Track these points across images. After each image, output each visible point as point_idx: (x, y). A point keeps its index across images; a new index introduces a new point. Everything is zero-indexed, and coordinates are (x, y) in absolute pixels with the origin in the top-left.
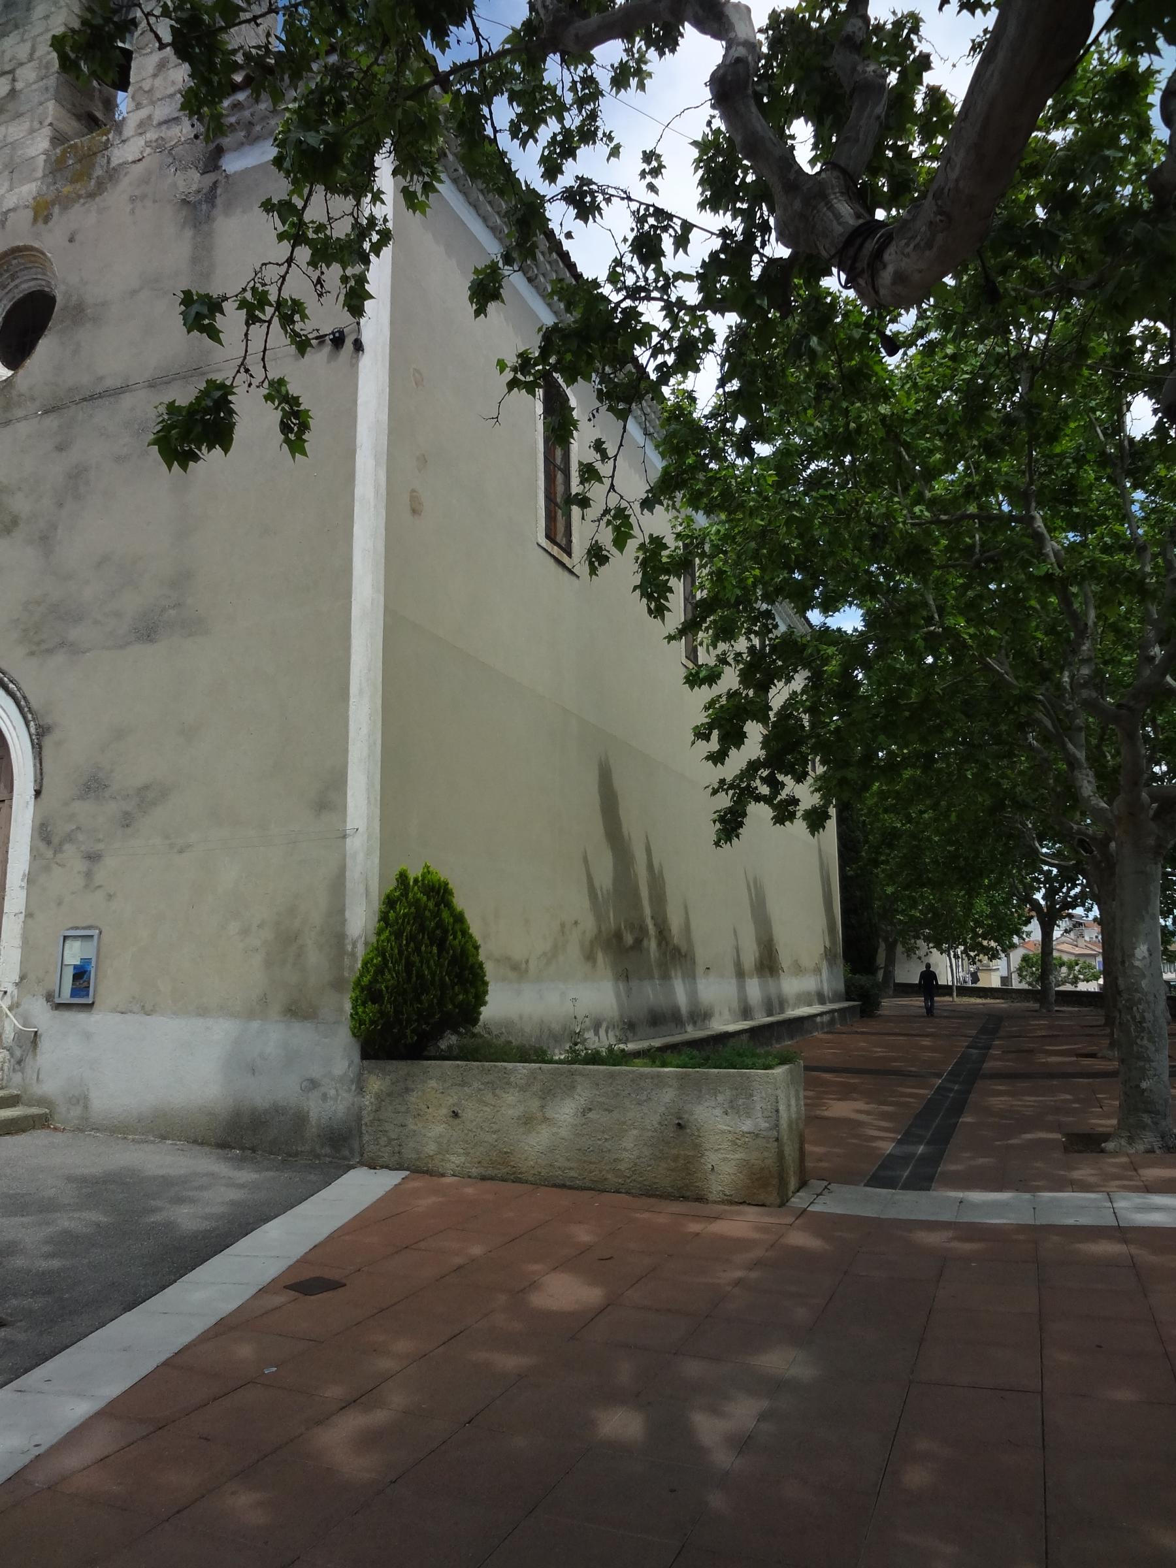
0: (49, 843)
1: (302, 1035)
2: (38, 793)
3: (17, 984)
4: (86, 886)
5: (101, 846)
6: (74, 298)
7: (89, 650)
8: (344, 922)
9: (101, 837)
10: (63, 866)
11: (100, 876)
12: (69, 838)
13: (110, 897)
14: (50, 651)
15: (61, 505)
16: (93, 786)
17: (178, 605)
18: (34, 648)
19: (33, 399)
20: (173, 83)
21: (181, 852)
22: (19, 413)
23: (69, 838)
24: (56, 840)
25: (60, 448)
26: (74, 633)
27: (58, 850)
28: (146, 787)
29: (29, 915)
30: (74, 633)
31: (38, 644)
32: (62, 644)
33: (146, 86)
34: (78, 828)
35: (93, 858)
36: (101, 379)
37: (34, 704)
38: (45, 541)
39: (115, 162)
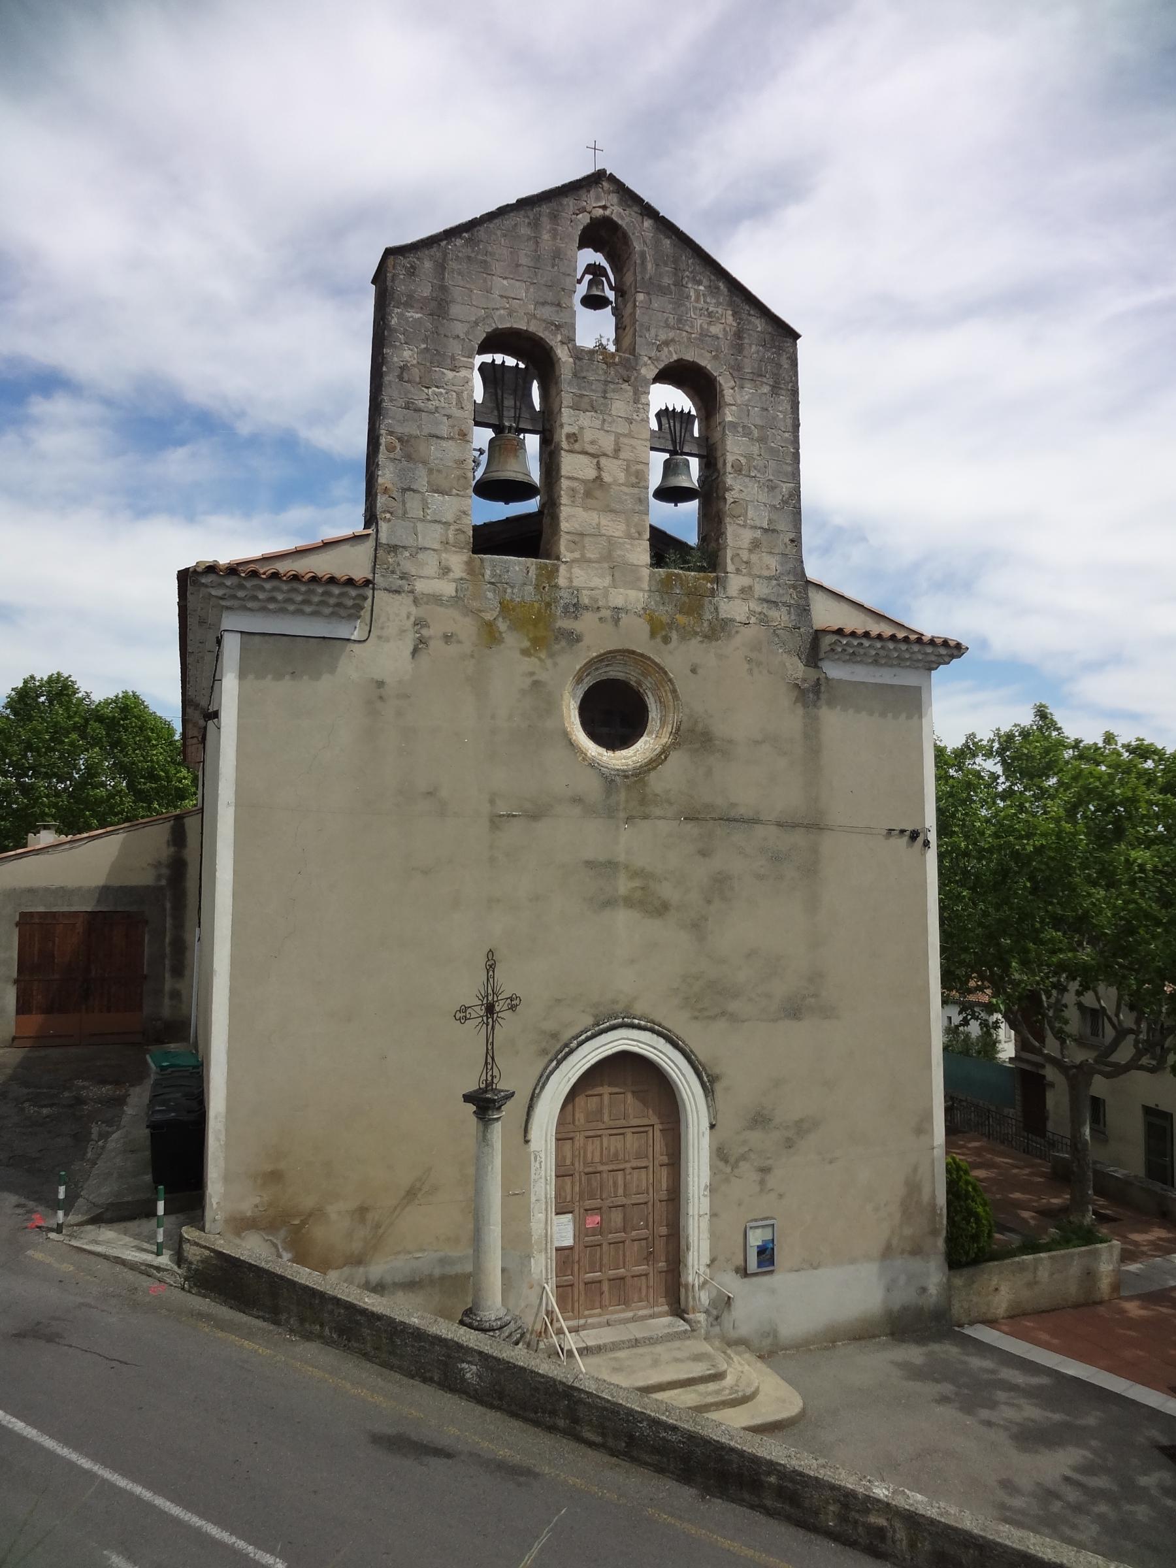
2: (712, 1126)
3: (708, 1266)
4: (762, 1190)
5: (770, 1162)
11: (771, 1181)
12: (743, 1157)
13: (781, 1196)
14: (713, 1018)
15: (709, 902)
16: (759, 1120)
17: (815, 996)
18: (697, 1014)
20: (768, 568)
21: (831, 1162)
22: (658, 812)
23: (743, 1157)
24: (732, 1160)
25: (704, 853)
26: (733, 1006)
27: (735, 1166)
28: (802, 1120)
29: (714, 1215)
30: (733, 1006)
31: (701, 1010)
32: (723, 1014)
35: (765, 1170)
36: (733, 805)
37: (701, 1058)
38: (697, 927)
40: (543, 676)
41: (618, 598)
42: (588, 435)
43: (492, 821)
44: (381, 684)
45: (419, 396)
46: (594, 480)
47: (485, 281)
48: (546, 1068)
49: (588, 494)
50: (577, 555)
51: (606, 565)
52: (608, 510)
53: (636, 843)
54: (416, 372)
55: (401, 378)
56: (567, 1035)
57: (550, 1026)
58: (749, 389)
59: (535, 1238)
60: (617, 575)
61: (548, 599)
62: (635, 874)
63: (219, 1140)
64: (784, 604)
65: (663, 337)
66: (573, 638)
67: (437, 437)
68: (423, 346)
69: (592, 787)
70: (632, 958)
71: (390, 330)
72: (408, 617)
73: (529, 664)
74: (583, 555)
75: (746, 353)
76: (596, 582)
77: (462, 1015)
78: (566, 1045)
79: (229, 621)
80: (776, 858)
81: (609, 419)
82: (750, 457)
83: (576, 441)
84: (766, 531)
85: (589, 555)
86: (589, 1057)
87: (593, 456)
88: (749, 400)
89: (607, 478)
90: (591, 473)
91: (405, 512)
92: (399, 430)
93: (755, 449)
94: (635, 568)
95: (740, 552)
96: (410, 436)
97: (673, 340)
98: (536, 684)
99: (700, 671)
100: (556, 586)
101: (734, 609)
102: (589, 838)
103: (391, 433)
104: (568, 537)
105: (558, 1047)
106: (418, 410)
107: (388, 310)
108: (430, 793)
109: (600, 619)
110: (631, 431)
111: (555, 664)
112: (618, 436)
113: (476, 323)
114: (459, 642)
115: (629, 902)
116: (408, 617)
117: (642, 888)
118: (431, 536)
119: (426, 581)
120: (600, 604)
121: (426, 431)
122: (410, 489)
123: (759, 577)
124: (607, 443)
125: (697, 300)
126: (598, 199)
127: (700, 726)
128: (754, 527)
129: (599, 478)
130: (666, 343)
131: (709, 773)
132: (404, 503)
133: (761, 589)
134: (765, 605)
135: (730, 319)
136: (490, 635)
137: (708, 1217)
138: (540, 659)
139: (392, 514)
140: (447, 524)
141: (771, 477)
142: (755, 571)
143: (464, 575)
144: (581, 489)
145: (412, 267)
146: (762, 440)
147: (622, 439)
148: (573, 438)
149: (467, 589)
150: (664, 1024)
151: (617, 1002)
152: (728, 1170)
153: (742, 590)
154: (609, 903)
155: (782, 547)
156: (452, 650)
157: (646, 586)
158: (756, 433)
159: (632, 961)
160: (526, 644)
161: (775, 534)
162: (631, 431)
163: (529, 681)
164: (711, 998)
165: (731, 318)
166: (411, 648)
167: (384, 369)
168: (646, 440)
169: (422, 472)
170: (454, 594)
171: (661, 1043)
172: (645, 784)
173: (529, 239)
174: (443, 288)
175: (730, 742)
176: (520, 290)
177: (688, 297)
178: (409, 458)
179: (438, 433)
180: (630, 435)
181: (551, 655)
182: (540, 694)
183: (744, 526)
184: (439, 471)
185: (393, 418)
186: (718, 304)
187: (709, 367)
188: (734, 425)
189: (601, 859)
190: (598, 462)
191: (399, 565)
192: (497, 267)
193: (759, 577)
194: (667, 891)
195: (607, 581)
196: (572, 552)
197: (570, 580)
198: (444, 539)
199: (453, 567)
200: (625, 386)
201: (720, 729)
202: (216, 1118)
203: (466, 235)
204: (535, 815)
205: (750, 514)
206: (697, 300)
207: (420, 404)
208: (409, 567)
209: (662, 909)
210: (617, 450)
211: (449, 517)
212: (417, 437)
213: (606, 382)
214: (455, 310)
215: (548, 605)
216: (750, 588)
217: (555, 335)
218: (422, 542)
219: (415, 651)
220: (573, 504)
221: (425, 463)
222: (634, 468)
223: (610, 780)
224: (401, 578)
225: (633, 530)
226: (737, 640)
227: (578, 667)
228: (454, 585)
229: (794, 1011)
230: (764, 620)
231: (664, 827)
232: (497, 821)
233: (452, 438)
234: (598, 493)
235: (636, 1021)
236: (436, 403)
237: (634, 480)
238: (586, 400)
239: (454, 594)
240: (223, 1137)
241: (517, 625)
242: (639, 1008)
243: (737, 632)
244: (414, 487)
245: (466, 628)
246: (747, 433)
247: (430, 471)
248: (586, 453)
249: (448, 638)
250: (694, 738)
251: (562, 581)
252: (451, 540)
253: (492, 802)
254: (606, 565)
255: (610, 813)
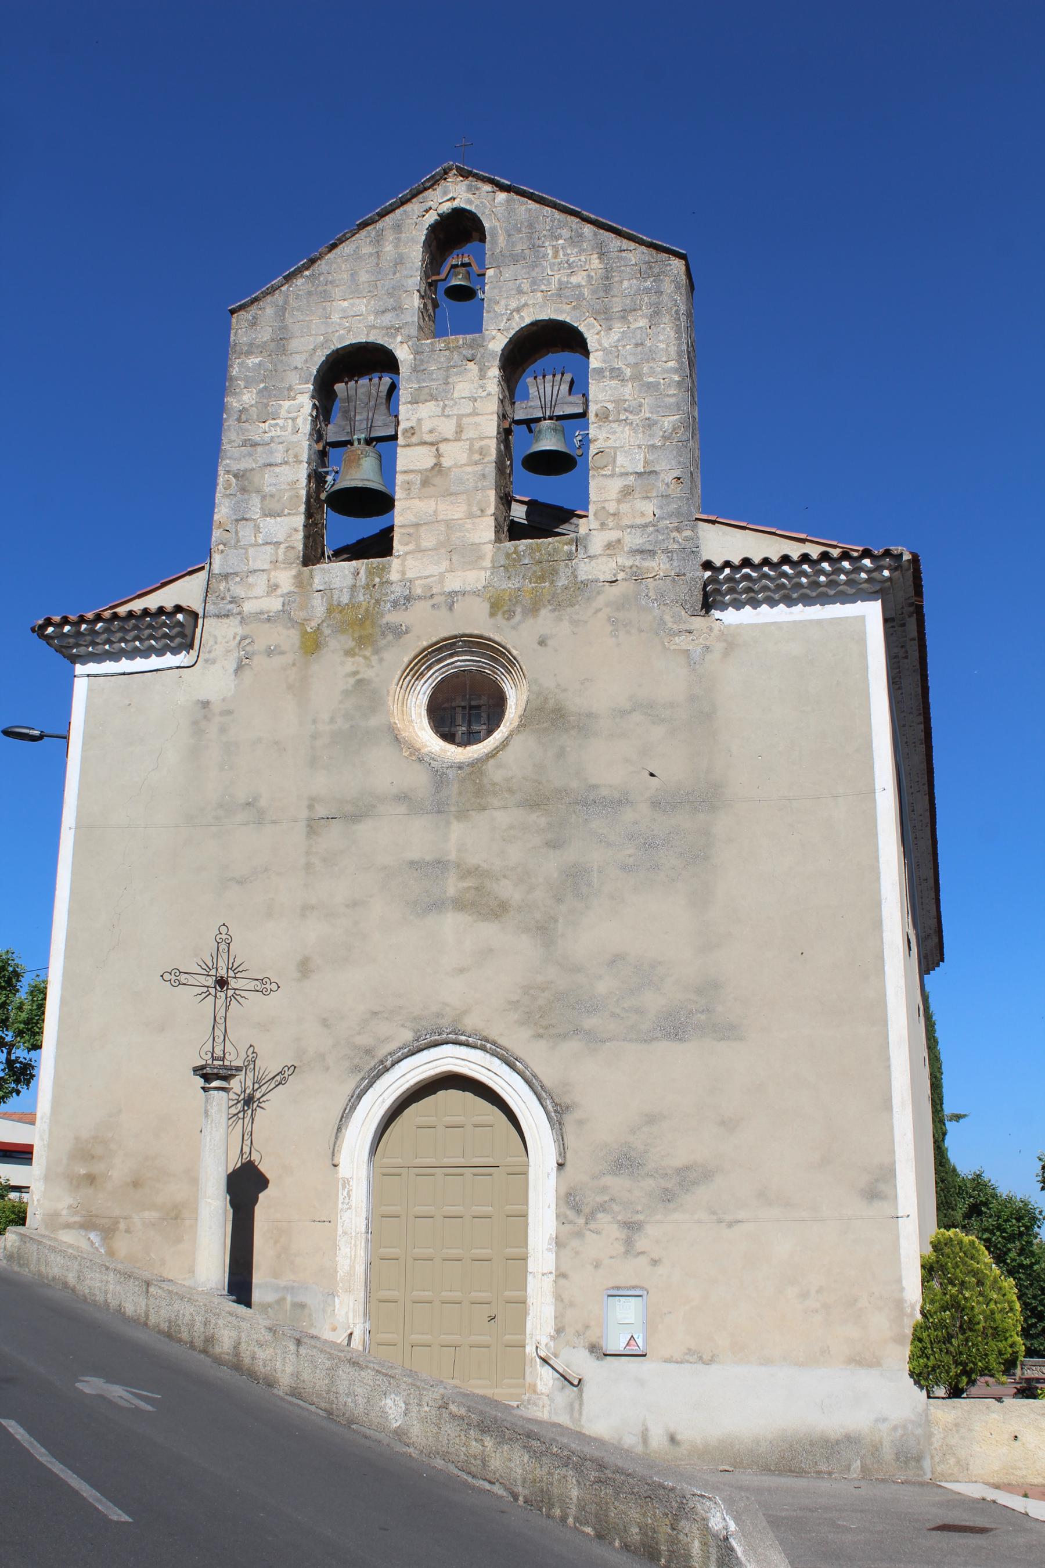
0: (579, 1212)
1: (866, 1380)
2: (560, 1165)
3: (552, 1338)
4: (627, 1252)
5: (641, 1217)
6: (551, 702)
7: (609, 1040)
8: (902, 1289)
9: (639, 1208)
10: (598, 1233)
11: (642, 1243)
12: (602, 1208)
13: (655, 1262)
14: (564, 1037)
15: (559, 900)
16: (625, 1162)
17: (707, 1011)
18: (541, 1031)
19: (510, 790)
20: (643, 514)
21: (731, 1224)
22: (496, 802)
23: (602, 1208)
24: (587, 1210)
25: (554, 845)
26: (590, 1022)
27: (591, 1217)
28: (687, 1168)
29: (561, 1275)
30: (590, 1022)
31: (546, 1028)
32: (576, 1031)
33: (612, 507)
34: (612, 1200)
35: (632, 1227)
36: (595, 787)
37: (546, 1082)
38: (544, 931)
39: (582, 576)
40: (368, 674)
41: (453, 583)
42: (426, 426)
43: (309, 826)
44: (206, 704)
45: (257, 431)
46: (433, 468)
47: (324, 309)
48: (357, 1087)
49: (425, 483)
50: (411, 547)
51: (443, 551)
52: (448, 494)
53: (470, 839)
54: (254, 411)
55: (239, 420)
56: (382, 1052)
57: (364, 1040)
58: (618, 328)
59: (340, 1274)
60: (455, 558)
61: (377, 596)
62: (469, 873)
63: (43, 1140)
64: (666, 551)
65: (514, 305)
66: (399, 632)
67: (271, 465)
68: (262, 385)
69: (418, 780)
70: (468, 968)
71: (231, 379)
72: (234, 638)
73: (349, 665)
74: (418, 545)
75: (615, 291)
76: (433, 570)
77: (175, 977)
78: (382, 1062)
79: (79, 669)
80: (649, 844)
81: (451, 403)
82: (617, 402)
83: (413, 434)
84: (639, 474)
85: (424, 544)
86: (408, 1076)
87: (432, 444)
88: (619, 340)
89: (446, 462)
90: (430, 462)
91: (238, 541)
92: (235, 467)
93: (628, 391)
94: (476, 546)
95: (606, 505)
96: (245, 471)
97: (526, 305)
98: (360, 682)
99: (550, 642)
100: (389, 582)
101: (596, 567)
102: (418, 837)
103: (228, 472)
104: (402, 530)
105: (372, 1064)
106: (255, 445)
107: (230, 363)
108: (248, 804)
109: (433, 606)
110: (475, 408)
111: (381, 660)
112: (460, 417)
113: (314, 350)
114: (283, 653)
115: (460, 904)
116: (234, 638)
117: (476, 889)
118: (260, 559)
119: (254, 600)
120: (434, 591)
121: (261, 461)
122: (241, 520)
123: (631, 527)
124: (447, 428)
125: (556, 256)
126: (445, 193)
127: (551, 703)
128: (622, 475)
129: (438, 465)
130: (518, 310)
131: (561, 754)
132: (237, 533)
133: (634, 540)
134: (638, 557)
135: (595, 262)
136: (312, 644)
137: (552, 1277)
138: (365, 658)
139: (224, 545)
140: (277, 544)
141: (648, 415)
142: (626, 521)
143: (292, 589)
144: (417, 479)
145: (254, 318)
146: (637, 377)
147: (465, 420)
148: (412, 431)
149: (294, 602)
150: (501, 1041)
151: (443, 1016)
152: (581, 1221)
153: (609, 546)
154: (437, 906)
155: (662, 487)
156: (278, 660)
157: (487, 563)
158: (628, 372)
159: (462, 971)
160: (351, 644)
161: (653, 476)
162: (475, 408)
163: (352, 681)
164: (557, 1011)
165: (597, 261)
166: (235, 666)
167: (225, 416)
168: (492, 413)
169: (256, 500)
170: (280, 608)
171: (496, 1064)
172: (481, 773)
173: (371, 254)
174: (284, 328)
175: (590, 715)
176: (361, 306)
177: (545, 255)
178: (243, 490)
179: (272, 461)
180: (475, 413)
181: (376, 652)
182: (365, 695)
183: (612, 476)
184: (272, 496)
185: (230, 458)
186: (581, 251)
187: (568, 320)
188: (600, 371)
189: (428, 858)
190: (437, 450)
191: (229, 590)
192: (337, 292)
193: (631, 527)
194: (507, 890)
195: (445, 565)
196: (407, 544)
197: (403, 573)
198: (274, 558)
199: (281, 584)
200: (471, 365)
201: (575, 703)
202: (42, 1118)
203: (307, 273)
204: (355, 817)
205: (620, 460)
206: (556, 256)
207: (257, 438)
208: (239, 591)
209: (498, 911)
210: (460, 430)
211: (281, 538)
212: (252, 470)
213: (448, 368)
214: (294, 344)
215: (377, 602)
216: (619, 541)
217: (394, 337)
218: (253, 565)
219: (239, 668)
220: (409, 497)
221: (258, 491)
222: (477, 445)
223: (439, 775)
224: (231, 602)
225: (475, 508)
226: (600, 601)
227: (406, 660)
228: (282, 599)
229: (675, 1028)
230: (638, 577)
231: (502, 818)
232: (314, 826)
233: (286, 463)
234: (437, 480)
235: (463, 1038)
236: (273, 434)
237: (477, 457)
238: (426, 390)
239: (280, 608)
240: (46, 1137)
241: (341, 629)
242: (472, 1022)
243: (598, 593)
244: (248, 516)
245: (287, 638)
246: (616, 374)
247: (264, 498)
248: (425, 443)
249: (269, 652)
250: (549, 717)
251: (394, 576)
252: (281, 557)
253: (311, 807)
254: (443, 551)
255: (440, 809)
